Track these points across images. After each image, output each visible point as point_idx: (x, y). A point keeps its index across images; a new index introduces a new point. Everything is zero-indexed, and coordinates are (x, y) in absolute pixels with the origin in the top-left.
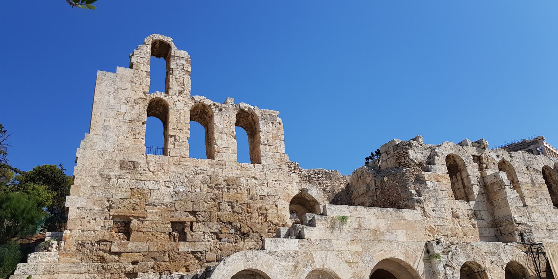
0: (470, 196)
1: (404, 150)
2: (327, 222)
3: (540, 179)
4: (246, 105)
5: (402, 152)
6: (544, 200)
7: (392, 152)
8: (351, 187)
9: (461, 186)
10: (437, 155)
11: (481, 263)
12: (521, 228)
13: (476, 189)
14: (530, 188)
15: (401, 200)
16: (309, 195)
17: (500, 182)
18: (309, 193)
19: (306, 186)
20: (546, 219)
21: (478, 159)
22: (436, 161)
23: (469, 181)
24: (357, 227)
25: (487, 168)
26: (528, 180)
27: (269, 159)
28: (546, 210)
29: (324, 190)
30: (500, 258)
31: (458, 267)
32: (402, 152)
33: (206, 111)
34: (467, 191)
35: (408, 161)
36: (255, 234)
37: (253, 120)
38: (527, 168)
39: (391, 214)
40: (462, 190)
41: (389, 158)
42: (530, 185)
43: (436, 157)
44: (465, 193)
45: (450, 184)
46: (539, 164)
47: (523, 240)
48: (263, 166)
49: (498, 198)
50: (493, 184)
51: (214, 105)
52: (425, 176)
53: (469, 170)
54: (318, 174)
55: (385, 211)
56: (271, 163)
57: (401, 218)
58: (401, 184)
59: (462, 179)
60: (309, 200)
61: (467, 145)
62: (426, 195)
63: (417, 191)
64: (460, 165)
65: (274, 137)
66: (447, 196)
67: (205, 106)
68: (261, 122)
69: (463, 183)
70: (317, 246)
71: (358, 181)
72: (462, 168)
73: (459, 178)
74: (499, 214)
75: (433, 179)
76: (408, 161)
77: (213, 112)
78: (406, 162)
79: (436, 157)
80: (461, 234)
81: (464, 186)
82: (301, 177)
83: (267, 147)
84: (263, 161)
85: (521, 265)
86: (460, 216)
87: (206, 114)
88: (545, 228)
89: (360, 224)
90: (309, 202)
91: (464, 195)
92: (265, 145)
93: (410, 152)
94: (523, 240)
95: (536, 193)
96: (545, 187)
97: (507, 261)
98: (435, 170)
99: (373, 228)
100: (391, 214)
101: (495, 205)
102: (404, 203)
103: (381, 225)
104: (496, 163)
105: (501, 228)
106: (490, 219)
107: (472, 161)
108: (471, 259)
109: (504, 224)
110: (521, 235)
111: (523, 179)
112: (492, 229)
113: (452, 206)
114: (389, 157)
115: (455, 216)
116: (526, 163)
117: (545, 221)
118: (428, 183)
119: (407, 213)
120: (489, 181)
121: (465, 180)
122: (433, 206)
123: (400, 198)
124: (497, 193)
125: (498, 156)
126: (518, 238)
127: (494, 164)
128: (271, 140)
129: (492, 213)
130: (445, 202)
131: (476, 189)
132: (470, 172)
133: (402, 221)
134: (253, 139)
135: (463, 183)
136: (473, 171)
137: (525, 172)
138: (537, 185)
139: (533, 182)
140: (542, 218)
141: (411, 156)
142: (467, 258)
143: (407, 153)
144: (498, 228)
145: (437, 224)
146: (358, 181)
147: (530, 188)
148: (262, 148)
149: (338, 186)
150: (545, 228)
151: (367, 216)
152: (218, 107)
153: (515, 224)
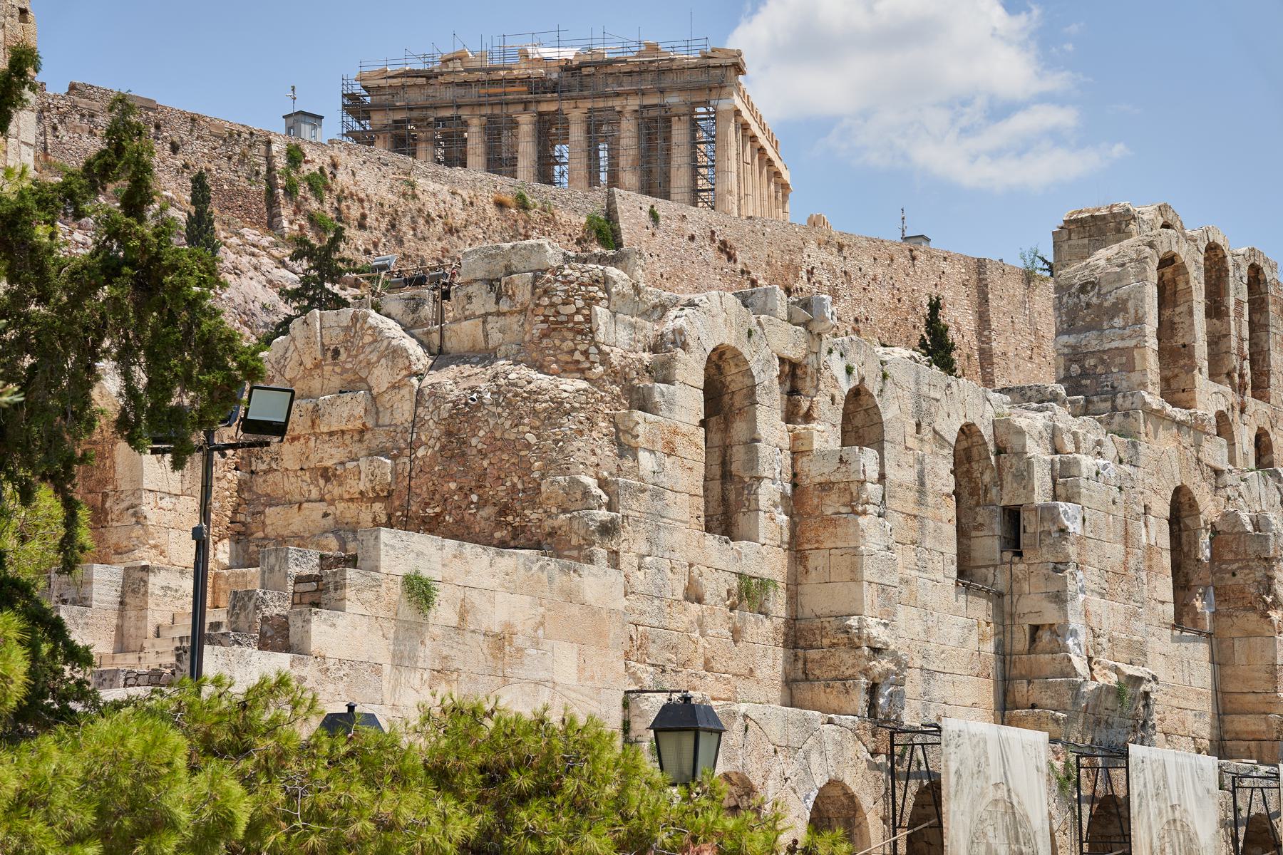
0: (741, 520)
1: (580, 303)
2: (378, 598)
6: (937, 557)
7: (524, 295)
9: (717, 471)
10: (684, 346)
11: (756, 782)
13: (770, 492)
15: (534, 505)
17: (853, 487)
20: (927, 631)
22: (679, 373)
23: (753, 460)
25: (808, 417)
26: (909, 476)
30: (807, 770)
34: (732, 497)
35: (586, 353)
38: (918, 425)
39: (551, 580)
40: (716, 486)
41: (499, 314)
42: (912, 495)
44: (724, 500)
45: (700, 470)
46: (954, 416)
49: (828, 544)
50: (826, 487)
52: (640, 429)
53: (762, 414)
55: (536, 567)
57: (570, 596)
59: (726, 449)
61: (772, 312)
62: (633, 507)
63: (602, 484)
64: (733, 387)
66: (686, 517)
69: (725, 463)
70: (341, 685)
72: (738, 401)
74: (817, 600)
75: (659, 446)
76: (586, 353)
78: (577, 356)
81: (726, 476)
85: (852, 797)
86: (707, 597)
94: (872, 706)
95: (922, 528)
96: (949, 511)
97: (820, 781)
98: (671, 404)
99: (497, 629)
100: (551, 580)
101: (811, 564)
102: (548, 524)
104: (838, 398)
105: (813, 654)
107: (776, 381)
109: (826, 642)
110: (873, 690)
111: (901, 474)
113: (693, 554)
114: (504, 306)
116: (918, 407)
117: (922, 636)
118: (644, 456)
119: (596, 582)
120: (814, 472)
121: (738, 454)
123: (533, 494)
124: (831, 522)
127: (833, 399)
129: (793, 598)
130: (677, 538)
132: (763, 429)
133: (575, 610)
135: (725, 463)
138: (930, 500)
139: (922, 484)
140: (918, 627)
141: (600, 337)
143: (588, 319)
144: (800, 652)
145: (642, 619)
147: (911, 508)
150: (918, 662)
151: (487, 583)
153: (866, 650)
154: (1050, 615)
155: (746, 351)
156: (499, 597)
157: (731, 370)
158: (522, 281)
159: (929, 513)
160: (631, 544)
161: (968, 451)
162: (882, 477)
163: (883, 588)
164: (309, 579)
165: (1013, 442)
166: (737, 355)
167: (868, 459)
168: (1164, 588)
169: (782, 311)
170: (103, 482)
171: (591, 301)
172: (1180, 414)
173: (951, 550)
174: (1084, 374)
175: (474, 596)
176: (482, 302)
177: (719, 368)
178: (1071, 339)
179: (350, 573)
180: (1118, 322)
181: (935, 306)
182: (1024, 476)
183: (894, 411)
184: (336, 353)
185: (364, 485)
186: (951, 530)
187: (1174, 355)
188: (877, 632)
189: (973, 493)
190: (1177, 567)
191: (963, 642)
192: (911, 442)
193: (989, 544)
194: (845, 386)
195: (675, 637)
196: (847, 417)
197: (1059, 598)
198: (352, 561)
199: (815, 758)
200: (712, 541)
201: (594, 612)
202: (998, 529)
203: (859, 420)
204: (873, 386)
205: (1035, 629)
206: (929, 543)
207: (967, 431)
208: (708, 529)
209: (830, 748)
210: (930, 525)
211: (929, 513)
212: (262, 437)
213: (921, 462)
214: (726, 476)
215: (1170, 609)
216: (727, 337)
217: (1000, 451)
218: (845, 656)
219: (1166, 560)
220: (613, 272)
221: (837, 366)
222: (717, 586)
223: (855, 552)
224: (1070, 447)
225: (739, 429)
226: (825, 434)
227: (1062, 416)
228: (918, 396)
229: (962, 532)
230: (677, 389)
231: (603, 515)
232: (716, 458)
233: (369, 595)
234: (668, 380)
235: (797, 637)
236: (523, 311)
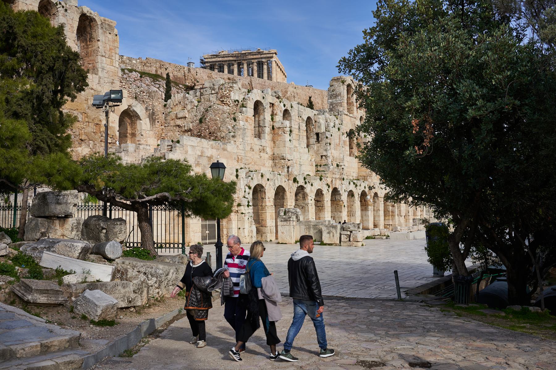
3: (303, 127)
4: (88, 9)
5: (226, 93)
8: (167, 108)
9: (257, 125)
10: (249, 100)
11: (264, 185)
12: (289, 163)
13: (268, 130)
14: (297, 133)
16: (134, 111)
18: (135, 109)
19: (133, 102)
21: (272, 105)
22: (248, 106)
24: (200, 154)
25: (276, 114)
26: (297, 127)
27: (105, 71)
28: (301, 151)
29: (146, 109)
30: (274, 183)
31: (252, 188)
32: (226, 93)
33: (49, 7)
36: (91, 142)
37: (91, 26)
40: (257, 129)
41: (212, 94)
42: (298, 130)
43: (249, 102)
44: (259, 131)
45: (253, 125)
47: (288, 171)
48: (100, 78)
51: (60, 3)
53: (266, 114)
54: (144, 92)
56: (106, 75)
57: (224, 150)
58: (222, 120)
59: (259, 121)
60: (132, 114)
62: (239, 133)
65: (110, 49)
67: (50, 3)
68: (100, 31)
69: (259, 124)
71: (177, 105)
73: (257, 119)
74: (277, 152)
77: (58, 11)
79: (249, 102)
80: (253, 163)
81: (259, 126)
82: (129, 92)
83: (104, 58)
84: (100, 73)
85: (284, 189)
87: (47, 10)
88: (298, 163)
89: (202, 152)
90: (132, 116)
91: (257, 133)
92: (102, 56)
93: (232, 94)
94: (288, 171)
96: (305, 134)
98: (247, 111)
103: (213, 154)
105: (276, 161)
106: (272, 153)
108: (260, 183)
110: (288, 167)
111: (295, 127)
112: (271, 162)
114: (213, 92)
115: (252, 149)
119: (230, 147)
120: (277, 125)
122: (241, 140)
125: (284, 105)
126: (286, 169)
128: (108, 53)
130: (249, 139)
131: (268, 130)
132: (266, 117)
133: (226, 152)
134: (87, 45)
135: (259, 124)
136: (267, 115)
137: (297, 120)
140: (299, 156)
141: (232, 98)
142: (258, 181)
146: (177, 105)
147: (297, 133)
148: (99, 58)
149: (157, 106)
151: (207, 147)
152: (63, 7)
154: (325, 154)
155: (263, 101)
156: (210, 149)
157: (259, 104)
158: (216, 87)
159: (301, 134)
160: (239, 140)
161: (309, 122)
162: (291, 127)
163: (290, 148)
164: (170, 146)
165: (318, 120)
166: (261, 102)
167: (287, 123)
168: (348, 148)
169: (270, 94)
170: (135, 128)
171: (230, 91)
172: (351, 115)
173: (305, 141)
174: (333, 107)
175: (205, 150)
176: (209, 91)
177: (258, 106)
178: (331, 101)
179: (177, 144)
180: (339, 97)
181: (310, 98)
182: (319, 127)
183: (294, 113)
184: (180, 103)
185: (186, 128)
186: (305, 137)
187: (349, 104)
188: (288, 157)
189: (310, 130)
190: (350, 145)
191: (307, 160)
192: (297, 120)
193: (313, 140)
194: (284, 109)
195: (248, 158)
196: (284, 115)
197: (326, 150)
198: (178, 142)
199: (276, 181)
200: (256, 139)
201: (230, 153)
202: (315, 137)
203: (287, 116)
204: (289, 109)
205: (322, 156)
206: (301, 140)
207: (309, 118)
208: (255, 137)
209: (279, 179)
210: (301, 136)
211: (301, 134)
212: (116, 104)
213: (299, 124)
214: (259, 126)
215: (348, 152)
216: (259, 99)
217: (316, 122)
218: (283, 161)
219: (348, 143)
220: (234, 85)
221: (282, 104)
222: (257, 148)
223: (285, 141)
224: (329, 121)
225: (262, 117)
226: (279, 117)
227: (327, 115)
228: (299, 111)
229: (308, 138)
230: (248, 109)
231: (232, 134)
232: (257, 123)
233: (181, 149)
234: (245, 107)
235: (274, 158)
236: (217, 93)
